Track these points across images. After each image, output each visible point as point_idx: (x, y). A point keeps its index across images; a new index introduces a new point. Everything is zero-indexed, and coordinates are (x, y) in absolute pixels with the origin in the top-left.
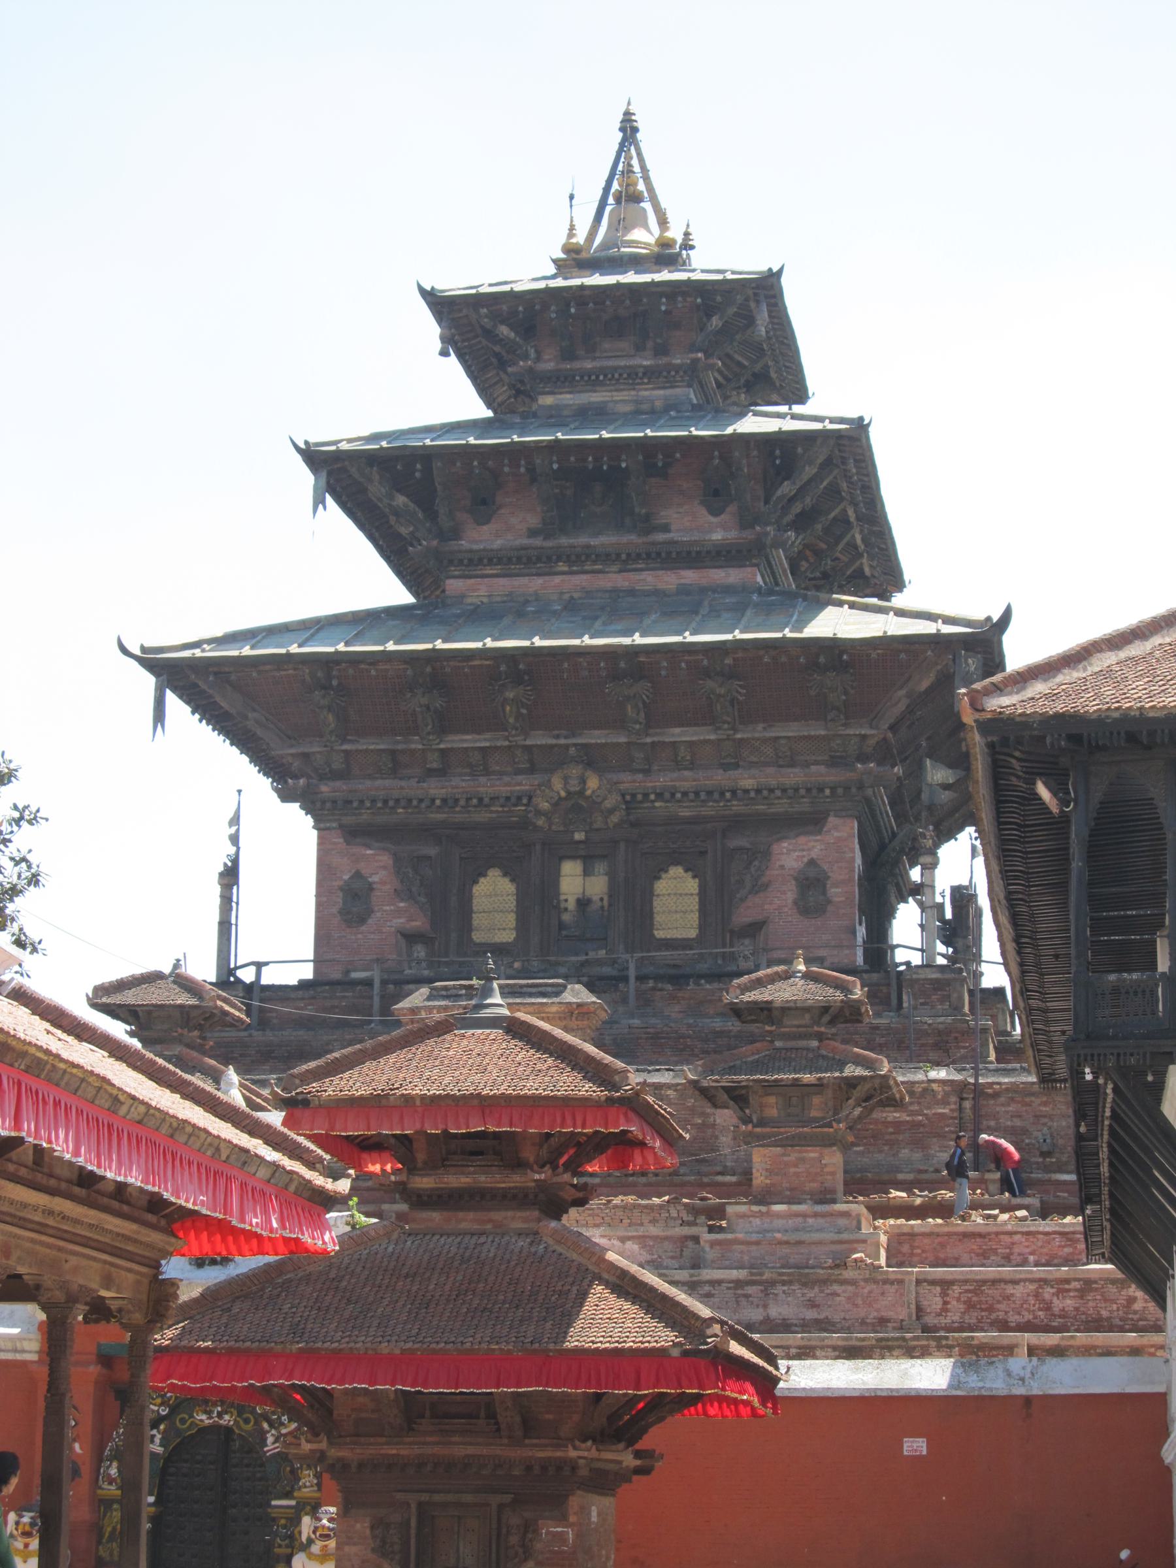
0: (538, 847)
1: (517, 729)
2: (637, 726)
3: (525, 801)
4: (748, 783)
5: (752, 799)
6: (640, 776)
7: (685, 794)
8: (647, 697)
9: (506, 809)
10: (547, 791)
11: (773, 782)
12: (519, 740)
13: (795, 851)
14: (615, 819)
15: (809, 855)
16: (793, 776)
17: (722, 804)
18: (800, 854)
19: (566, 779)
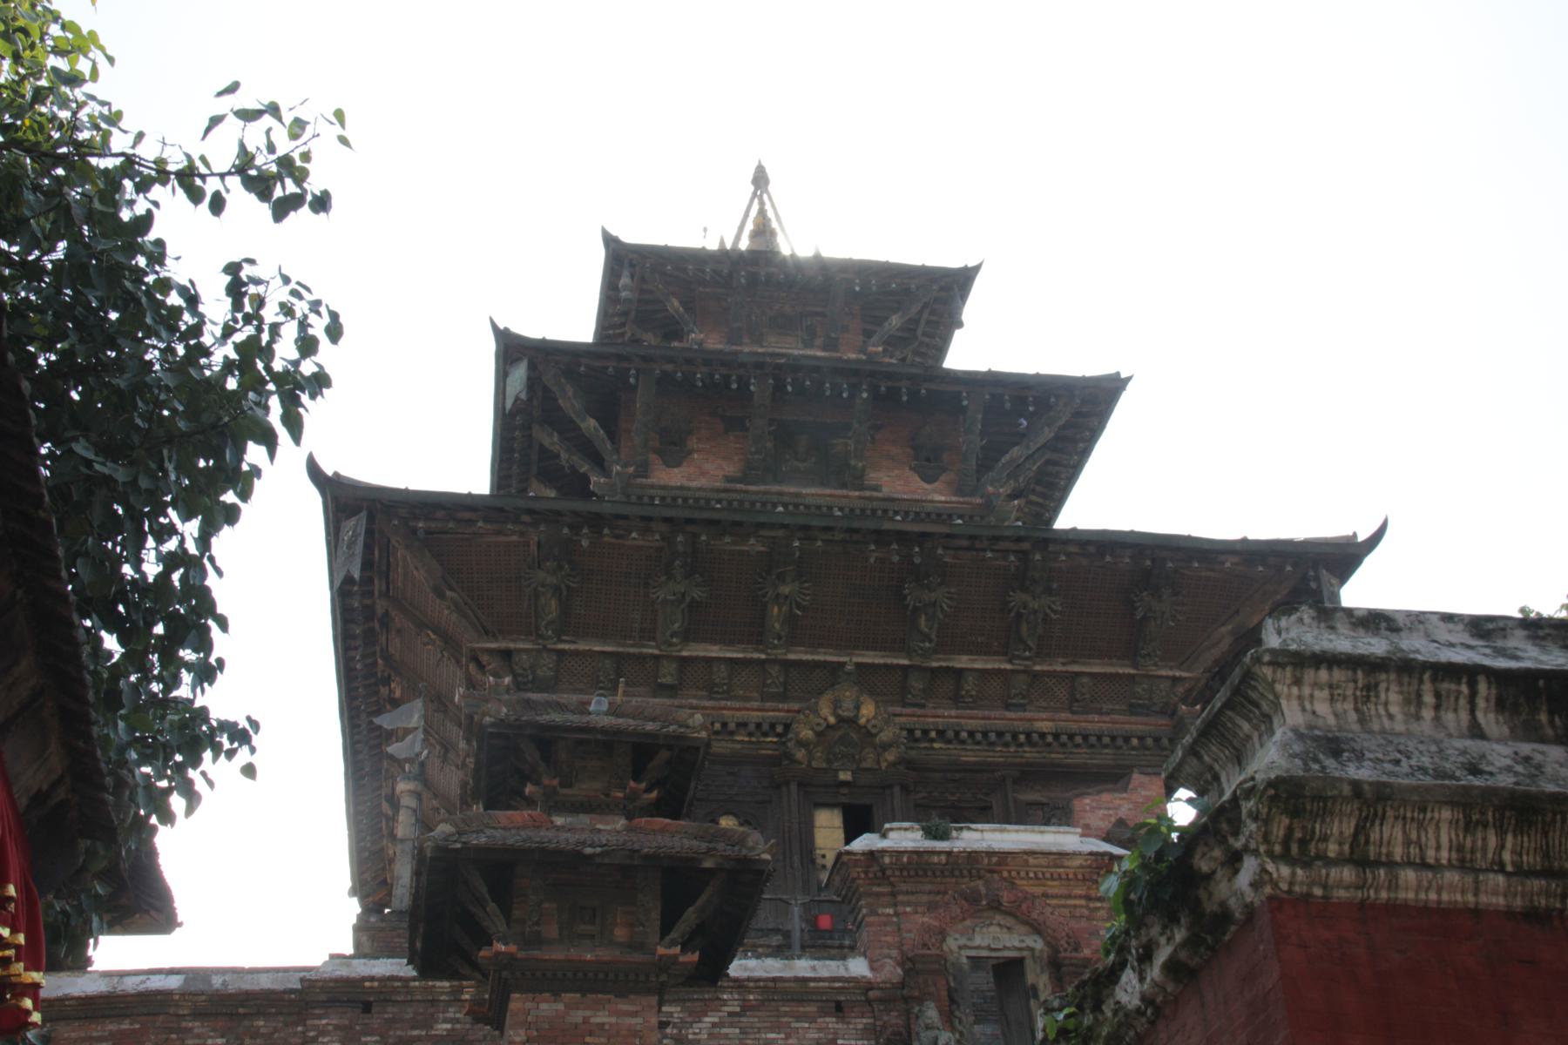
0: (794, 787)
1: (779, 638)
2: (927, 644)
3: (779, 729)
4: (1045, 726)
5: (1049, 745)
6: (919, 711)
7: (971, 734)
8: (950, 607)
9: (754, 739)
10: (811, 716)
11: (1074, 727)
12: (779, 653)
13: (1100, 808)
14: (891, 756)
15: (1117, 814)
16: (1094, 723)
17: (1012, 749)
18: (1106, 812)
19: (836, 705)
